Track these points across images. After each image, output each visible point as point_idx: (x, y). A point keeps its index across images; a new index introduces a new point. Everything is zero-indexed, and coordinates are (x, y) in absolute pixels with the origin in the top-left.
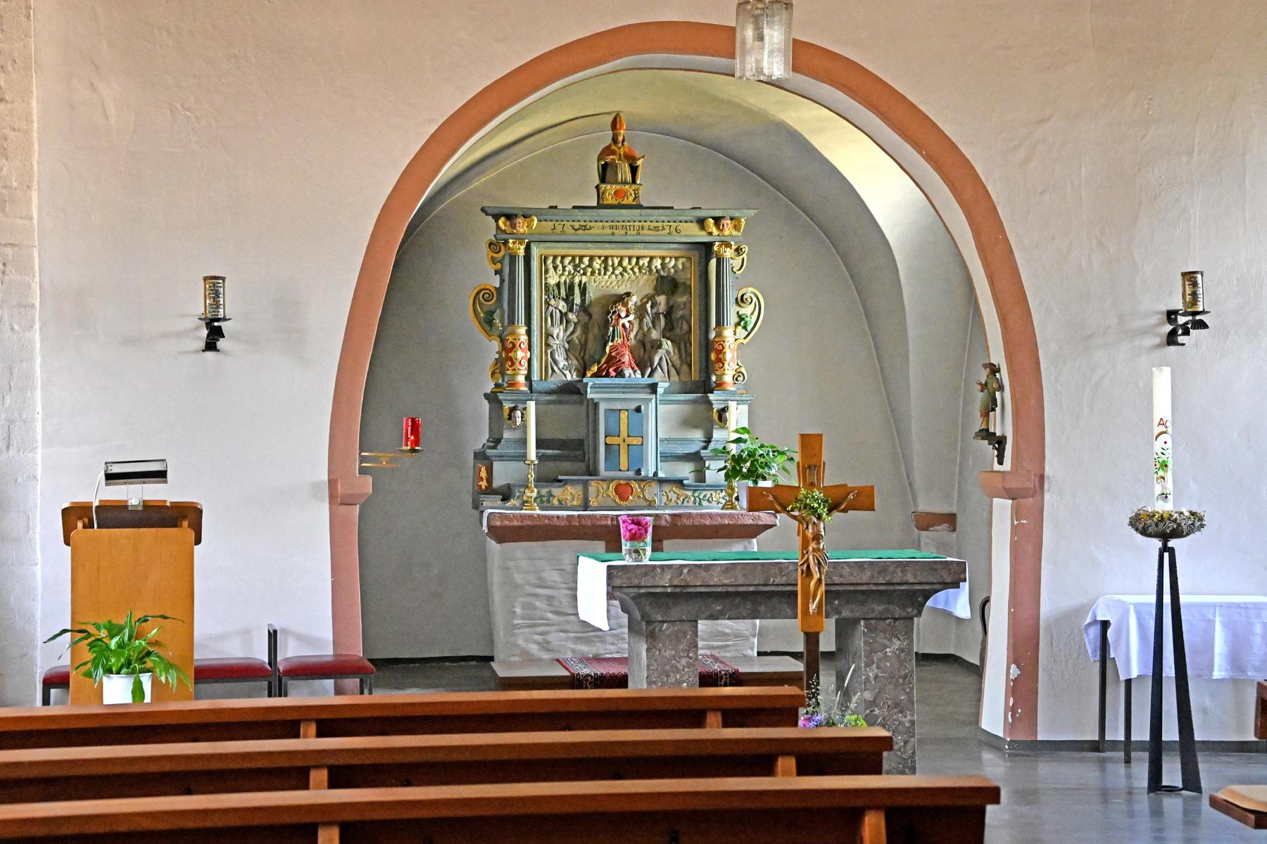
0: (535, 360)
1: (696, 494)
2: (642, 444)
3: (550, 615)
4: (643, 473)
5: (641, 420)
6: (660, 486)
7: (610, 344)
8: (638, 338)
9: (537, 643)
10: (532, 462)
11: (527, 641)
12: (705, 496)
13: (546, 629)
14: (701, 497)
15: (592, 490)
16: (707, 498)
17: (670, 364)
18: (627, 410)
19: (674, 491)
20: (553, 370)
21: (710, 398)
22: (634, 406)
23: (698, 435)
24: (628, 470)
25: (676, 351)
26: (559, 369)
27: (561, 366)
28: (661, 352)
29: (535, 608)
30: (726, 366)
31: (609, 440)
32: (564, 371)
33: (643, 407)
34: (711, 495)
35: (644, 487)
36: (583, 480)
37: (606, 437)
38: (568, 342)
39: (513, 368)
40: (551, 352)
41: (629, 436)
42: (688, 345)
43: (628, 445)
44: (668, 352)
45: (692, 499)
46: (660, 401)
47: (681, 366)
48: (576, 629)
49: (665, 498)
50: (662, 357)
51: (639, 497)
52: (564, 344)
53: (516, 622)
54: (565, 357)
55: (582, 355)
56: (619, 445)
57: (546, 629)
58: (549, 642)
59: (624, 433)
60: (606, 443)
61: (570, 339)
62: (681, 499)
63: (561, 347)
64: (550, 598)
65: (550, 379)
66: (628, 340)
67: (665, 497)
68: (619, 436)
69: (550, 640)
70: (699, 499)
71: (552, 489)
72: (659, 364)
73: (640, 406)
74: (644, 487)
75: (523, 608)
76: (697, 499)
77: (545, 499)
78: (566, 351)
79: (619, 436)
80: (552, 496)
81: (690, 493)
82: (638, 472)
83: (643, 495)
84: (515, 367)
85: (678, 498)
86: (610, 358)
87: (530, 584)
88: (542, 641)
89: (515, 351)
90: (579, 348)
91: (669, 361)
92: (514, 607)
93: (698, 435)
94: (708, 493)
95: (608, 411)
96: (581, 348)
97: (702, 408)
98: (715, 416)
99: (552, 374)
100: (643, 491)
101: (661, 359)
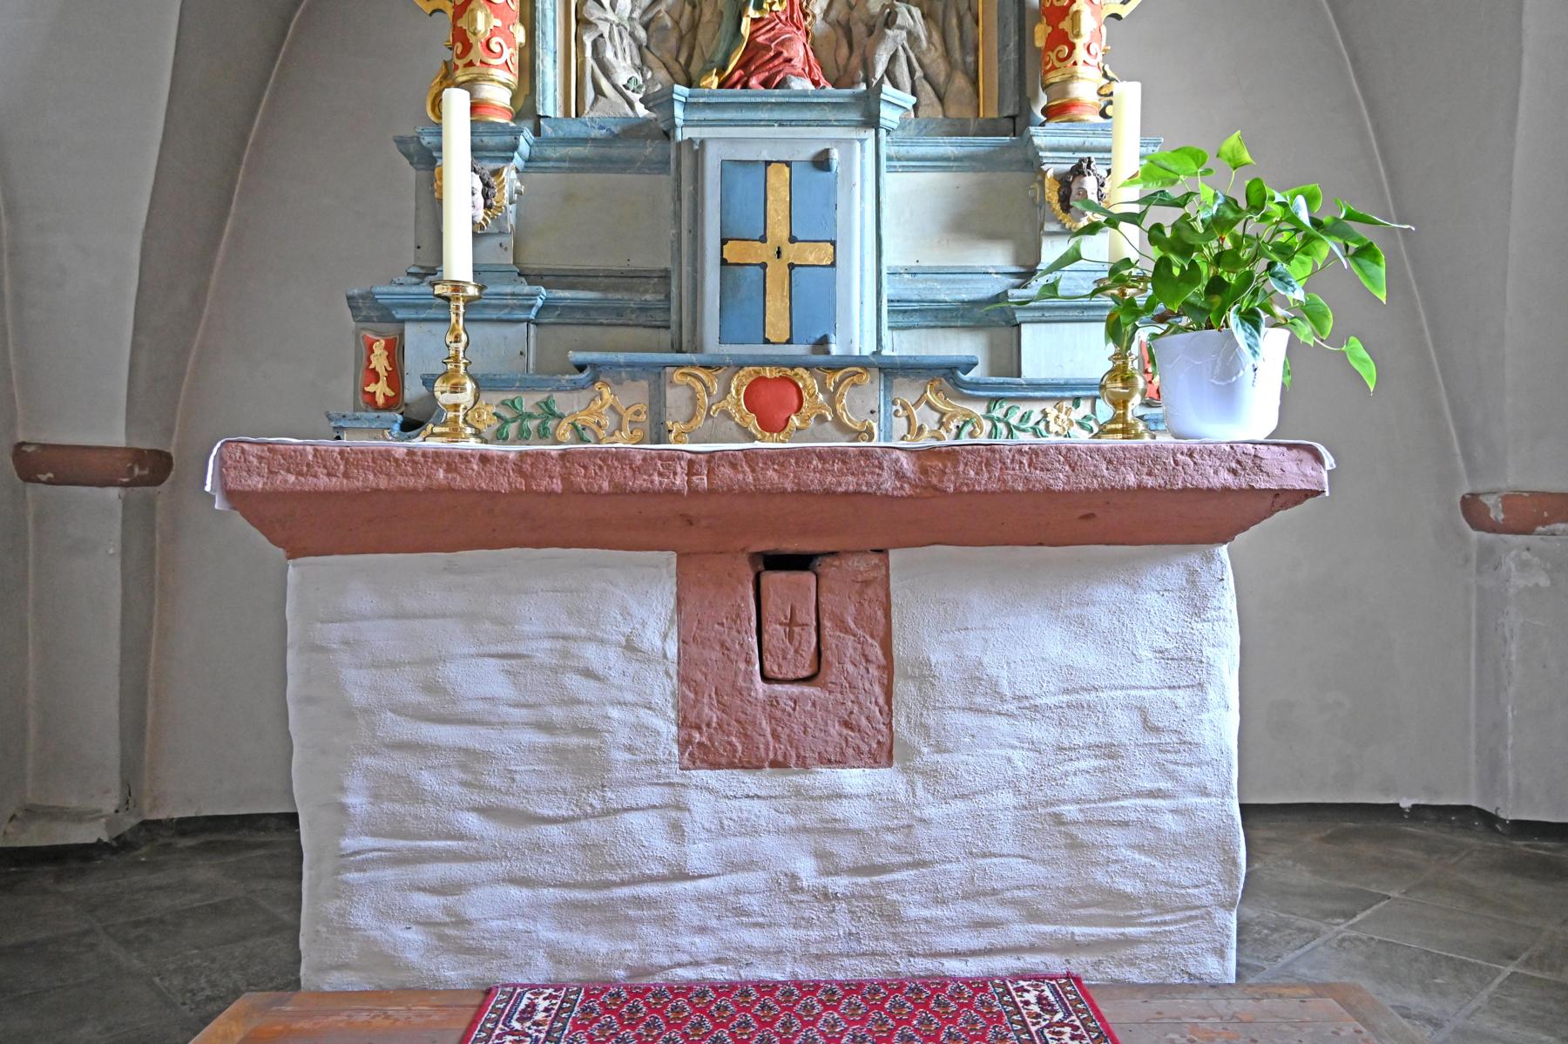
0: (549, 60)
1: (998, 413)
2: (833, 265)
3: (472, 822)
4: (835, 350)
5: (832, 190)
6: (888, 388)
7: (752, 13)
8: (833, 14)
9: (427, 923)
10: (457, 286)
11: (385, 914)
12: (1025, 418)
13: (457, 870)
14: (1014, 420)
15: (675, 397)
16: (1031, 423)
17: (919, 73)
18: (788, 164)
19: (928, 403)
20: (598, 91)
21: (1037, 141)
22: (809, 152)
23: (997, 258)
24: (789, 342)
25: (936, 37)
26: (615, 87)
27: (621, 80)
28: (895, 37)
29: (416, 795)
30: (1080, 54)
31: (733, 252)
32: (629, 93)
33: (835, 155)
34: (1045, 414)
35: (837, 386)
36: (646, 367)
37: (724, 242)
38: (646, 27)
39: (466, 60)
40: (595, 44)
41: (792, 240)
42: (968, 19)
43: (792, 266)
44: (912, 37)
45: (987, 425)
46: (889, 159)
47: (949, 77)
48: (564, 872)
49: (900, 424)
50: (897, 50)
51: (821, 419)
52: (633, 28)
53: (349, 843)
54: (638, 62)
55: (682, 60)
56: (764, 266)
57: (457, 870)
58: (461, 922)
59: (778, 230)
60: (724, 262)
61: (650, 15)
62: (952, 426)
63: (625, 35)
64: (470, 758)
65: (588, 114)
66: (805, 15)
67: (904, 421)
68: (763, 239)
69: (472, 913)
70: (1008, 424)
71: (556, 396)
72: (889, 73)
73: (827, 151)
74: (837, 386)
75: (376, 797)
76: (1001, 426)
77: (532, 424)
78: (640, 48)
79: (763, 239)
80: (553, 414)
81: (979, 409)
82: (822, 343)
83: (835, 411)
84: (471, 56)
85: (941, 424)
86: (753, 49)
87: (400, 710)
88: (440, 917)
89: (472, 10)
90: (672, 41)
91: (916, 65)
92: (343, 789)
93: (997, 258)
94: (1036, 410)
95: (728, 166)
96: (681, 38)
97: (1016, 178)
98: (1052, 195)
99: (596, 100)
100: (832, 400)
101: (893, 59)
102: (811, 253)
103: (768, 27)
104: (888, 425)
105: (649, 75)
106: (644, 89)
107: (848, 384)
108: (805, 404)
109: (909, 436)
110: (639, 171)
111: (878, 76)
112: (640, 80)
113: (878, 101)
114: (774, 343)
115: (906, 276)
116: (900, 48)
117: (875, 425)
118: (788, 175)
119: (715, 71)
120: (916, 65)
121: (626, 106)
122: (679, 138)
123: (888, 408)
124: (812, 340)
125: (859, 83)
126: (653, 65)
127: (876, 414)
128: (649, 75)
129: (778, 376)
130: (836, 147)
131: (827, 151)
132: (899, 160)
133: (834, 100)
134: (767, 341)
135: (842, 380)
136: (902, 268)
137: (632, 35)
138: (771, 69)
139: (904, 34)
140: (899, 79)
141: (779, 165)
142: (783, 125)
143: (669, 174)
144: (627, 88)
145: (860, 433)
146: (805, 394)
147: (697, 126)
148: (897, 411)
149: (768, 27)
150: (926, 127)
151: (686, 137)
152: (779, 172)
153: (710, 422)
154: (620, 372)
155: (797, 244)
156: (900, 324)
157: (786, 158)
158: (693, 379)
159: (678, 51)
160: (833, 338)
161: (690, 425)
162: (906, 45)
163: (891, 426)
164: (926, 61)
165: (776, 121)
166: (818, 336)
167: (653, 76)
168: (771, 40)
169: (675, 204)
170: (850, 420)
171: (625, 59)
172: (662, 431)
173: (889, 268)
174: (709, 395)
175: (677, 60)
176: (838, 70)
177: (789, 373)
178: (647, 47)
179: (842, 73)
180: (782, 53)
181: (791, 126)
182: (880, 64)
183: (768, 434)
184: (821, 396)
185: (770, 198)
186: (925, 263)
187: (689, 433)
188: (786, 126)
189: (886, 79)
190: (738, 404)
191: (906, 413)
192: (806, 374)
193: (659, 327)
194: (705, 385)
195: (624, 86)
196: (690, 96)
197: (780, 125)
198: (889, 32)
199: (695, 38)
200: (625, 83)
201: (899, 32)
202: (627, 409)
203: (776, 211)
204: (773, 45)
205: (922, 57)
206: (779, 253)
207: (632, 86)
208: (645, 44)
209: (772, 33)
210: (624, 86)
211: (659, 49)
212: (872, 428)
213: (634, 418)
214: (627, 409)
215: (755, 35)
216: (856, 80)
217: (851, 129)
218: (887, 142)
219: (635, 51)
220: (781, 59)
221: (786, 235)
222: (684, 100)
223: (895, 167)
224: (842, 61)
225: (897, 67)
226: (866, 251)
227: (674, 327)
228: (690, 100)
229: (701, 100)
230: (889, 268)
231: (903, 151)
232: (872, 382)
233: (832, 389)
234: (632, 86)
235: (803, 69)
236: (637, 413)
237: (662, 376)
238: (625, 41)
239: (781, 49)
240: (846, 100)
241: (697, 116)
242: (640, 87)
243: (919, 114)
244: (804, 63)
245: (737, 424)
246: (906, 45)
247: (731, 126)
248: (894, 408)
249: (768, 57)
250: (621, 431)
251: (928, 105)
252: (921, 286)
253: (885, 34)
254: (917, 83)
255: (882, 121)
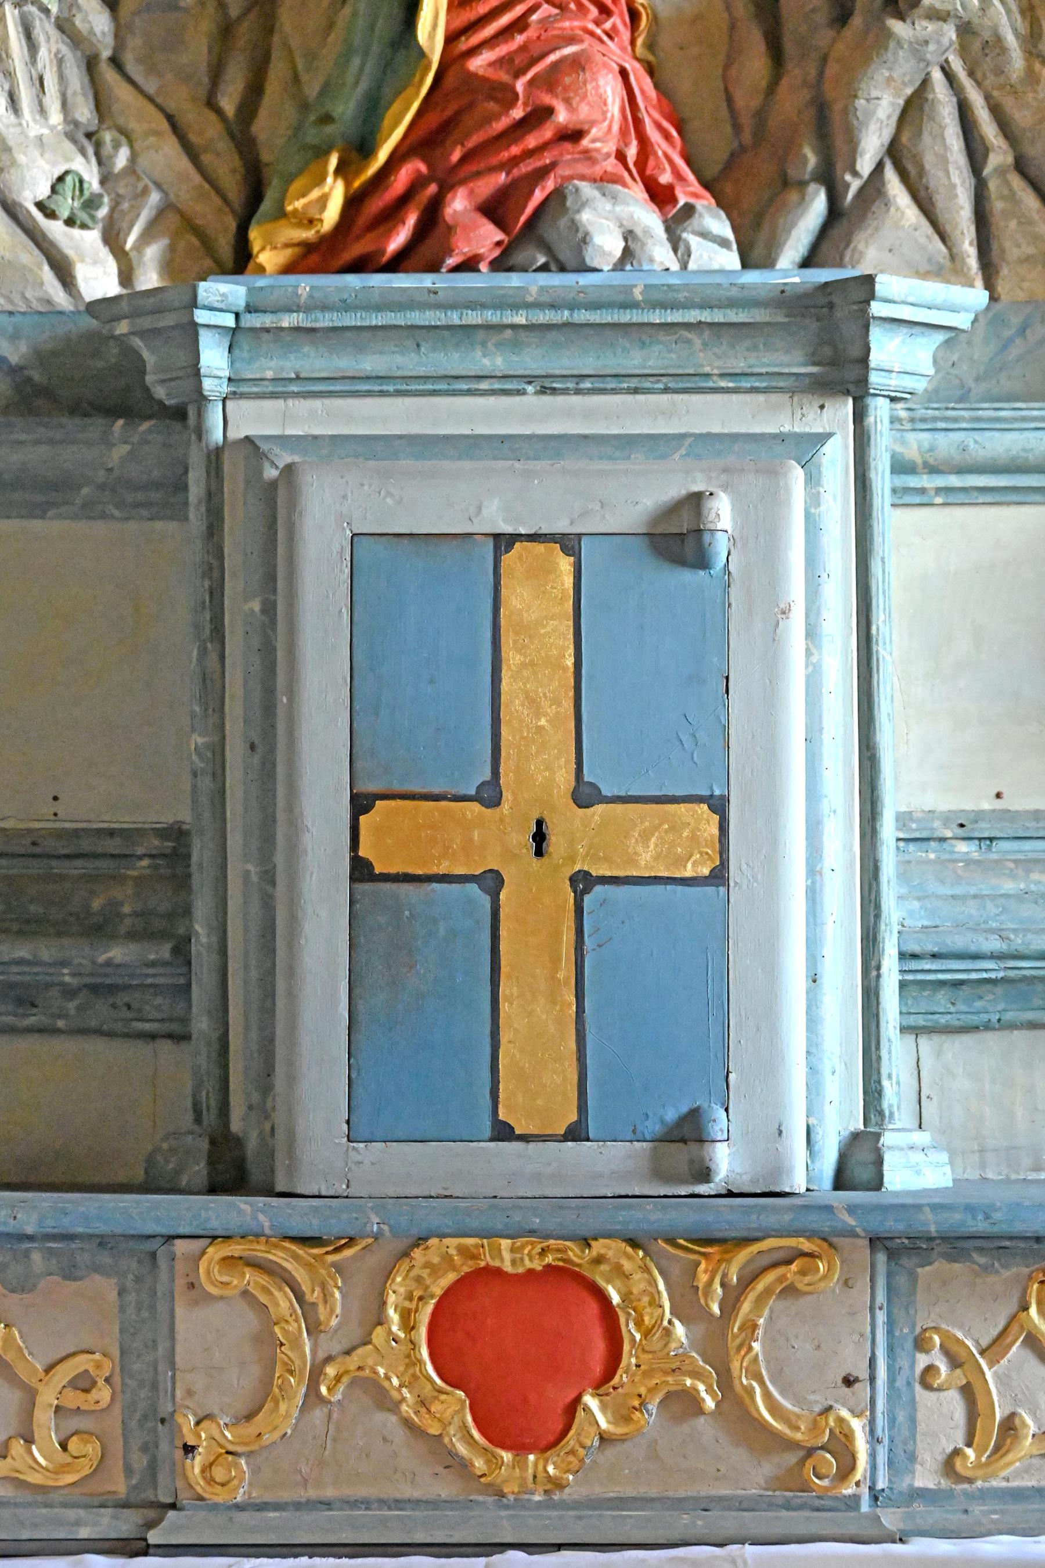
2: (719, 876)
17: (999, 156)
24: (575, 1133)
32: (55, 229)
37: (361, 804)
46: (900, 467)
50: (926, 82)
54: (85, 113)
55: (229, 104)
63: (45, 31)
67: (953, 1403)
73: (696, 501)
78: (91, 65)
83: (725, 1381)
91: (988, 128)
96: (226, 31)
102: (645, 836)
103: (505, 20)
104: (901, 1417)
105: (122, 159)
106: (103, 212)
107: (768, 1292)
108: (629, 1359)
109: (970, 1452)
110: (90, 511)
111: (865, 166)
112: (93, 183)
113: (865, 323)
114: (525, 1138)
115: (963, 847)
116: (937, 75)
117: (857, 1425)
118: (569, 581)
119: (333, 161)
120: (988, 128)
121: (47, 274)
122: (217, 435)
123: (903, 1362)
124: (653, 1127)
125: (802, 184)
126: (132, 125)
127: (863, 1390)
128: (122, 159)
129: (537, 1265)
130: (725, 488)
131: (696, 501)
132: (933, 470)
133: (718, 316)
134: (503, 1132)
135: (748, 1280)
136: (947, 818)
137: (64, 26)
138: (515, 161)
139: (950, 32)
140: (935, 177)
141: (539, 548)
142: (554, 391)
143: (180, 514)
144: (51, 215)
145: (810, 1452)
146: (631, 1331)
147: (273, 396)
148: (930, 1369)
149: (505, 20)
150: (1022, 331)
151: (236, 433)
152: (546, 571)
153: (318, 1414)
154: (27, 1254)
155: (599, 808)
156: (943, 1020)
157: (561, 526)
158: (263, 1279)
159: (216, 73)
160: (719, 1122)
161: (250, 1429)
162: (957, 66)
163: (913, 1420)
164: (1021, 117)
165: (530, 379)
166: (671, 1115)
167: (133, 158)
168: (515, 65)
169: (203, 652)
170: (774, 1408)
171: (42, 111)
172: (164, 1446)
173: (903, 819)
174: (314, 1329)
175: (211, 104)
176: (737, 127)
177: (575, 1253)
178: (115, 61)
179: (747, 137)
180: (549, 112)
181: (578, 392)
182: (873, 127)
183: (507, 1456)
184: (679, 1330)
185: (511, 658)
186: (1018, 802)
187: (249, 1455)
188: (565, 392)
189: (890, 174)
190: (412, 1361)
191: (960, 1377)
192: (631, 1260)
193: (152, 1037)
194: (300, 1297)
195: (40, 205)
196: (250, 309)
197: (543, 391)
198: (897, 26)
199: (268, 28)
200: (43, 191)
201: (931, 27)
202: (48, 1370)
203: (532, 701)
204: (520, 86)
205: (1008, 103)
206: (540, 837)
207: (66, 205)
208: (106, 53)
209: (520, 39)
210: (40, 205)
211: (152, 69)
212: (848, 1436)
213: (73, 1399)
214: (48, 1370)
215: (464, 44)
216: (792, 173)
217: (774, 398)
218: (894, 420)
219: (76, 79)
220: (547, 133)
221: (564, 778)
222: (230, 321)
223: (923, 491)
224: (747, 101)
225: (926, 139)
226: (825, 807)
227: (201, 1024)
228: (251, 321)
229: (287, 321)
230: (903, 819)
231: (946, 444)
232: (846, 1283)
233: (716, 1309)
234: (66, 205)
235: (621, 157)
236: (84, 1384)
237: (162, 1262)
238: (44, 54)
239: (547, 99)
240: (758, 315)
241: (268, 367)
242: (91, 204)
243: (1001, 288)
244: (624, 132)
245: (407, 1423)
246: (957, 66)
247: (383, 394)
248: (922, 1361)
249: (502, 124)
250: (29, 1441)
251: (1028, 259)
252: (1009, 886)
253: (889, 34)
254: (993, 185)
255: (874, 378)
